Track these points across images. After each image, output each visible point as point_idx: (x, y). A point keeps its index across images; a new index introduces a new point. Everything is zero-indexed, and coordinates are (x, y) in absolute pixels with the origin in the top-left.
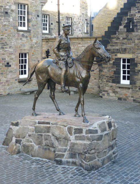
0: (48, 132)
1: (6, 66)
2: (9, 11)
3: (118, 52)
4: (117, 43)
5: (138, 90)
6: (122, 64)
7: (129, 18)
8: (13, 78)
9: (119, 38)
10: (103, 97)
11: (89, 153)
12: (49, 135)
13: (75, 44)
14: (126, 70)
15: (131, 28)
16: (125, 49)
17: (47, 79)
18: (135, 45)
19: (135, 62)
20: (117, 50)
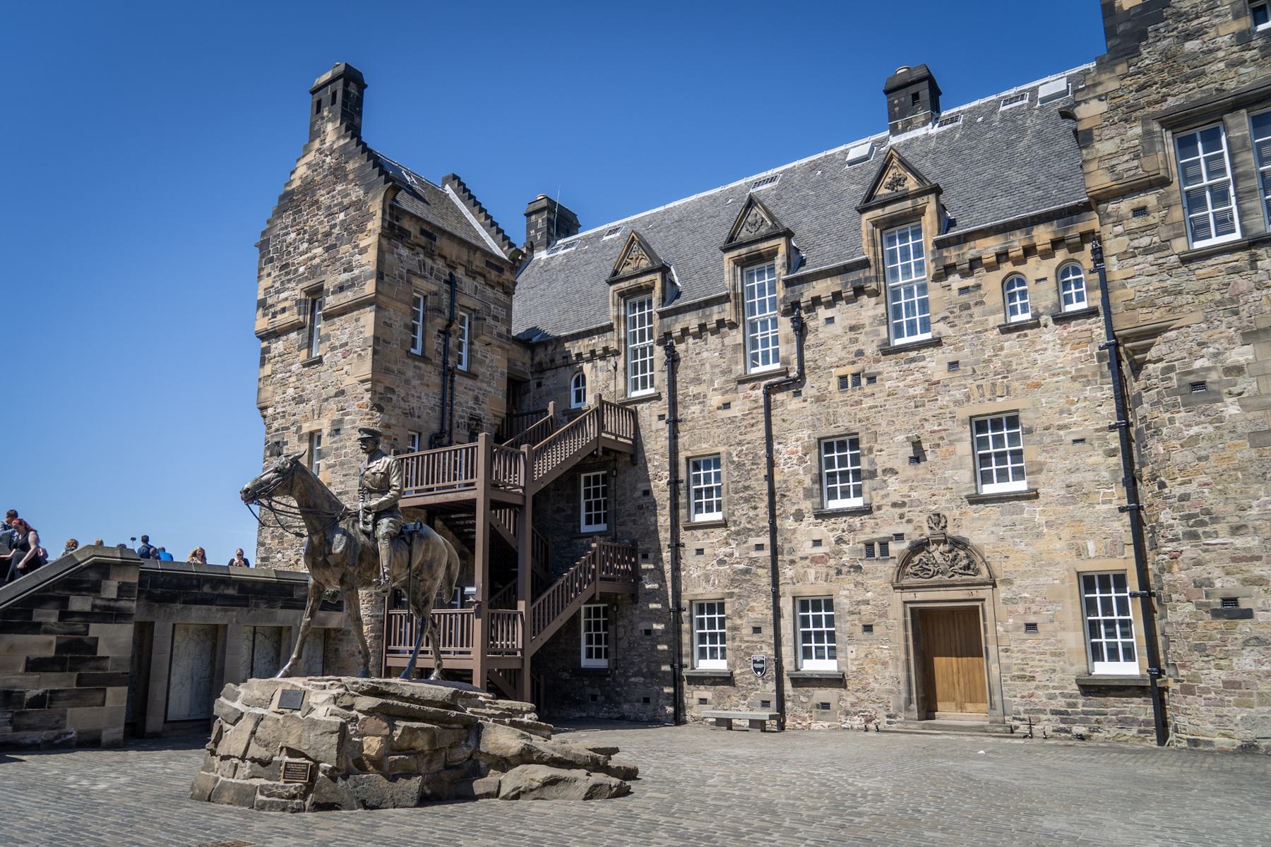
1: (1216, 614)
2: (1213, 376)
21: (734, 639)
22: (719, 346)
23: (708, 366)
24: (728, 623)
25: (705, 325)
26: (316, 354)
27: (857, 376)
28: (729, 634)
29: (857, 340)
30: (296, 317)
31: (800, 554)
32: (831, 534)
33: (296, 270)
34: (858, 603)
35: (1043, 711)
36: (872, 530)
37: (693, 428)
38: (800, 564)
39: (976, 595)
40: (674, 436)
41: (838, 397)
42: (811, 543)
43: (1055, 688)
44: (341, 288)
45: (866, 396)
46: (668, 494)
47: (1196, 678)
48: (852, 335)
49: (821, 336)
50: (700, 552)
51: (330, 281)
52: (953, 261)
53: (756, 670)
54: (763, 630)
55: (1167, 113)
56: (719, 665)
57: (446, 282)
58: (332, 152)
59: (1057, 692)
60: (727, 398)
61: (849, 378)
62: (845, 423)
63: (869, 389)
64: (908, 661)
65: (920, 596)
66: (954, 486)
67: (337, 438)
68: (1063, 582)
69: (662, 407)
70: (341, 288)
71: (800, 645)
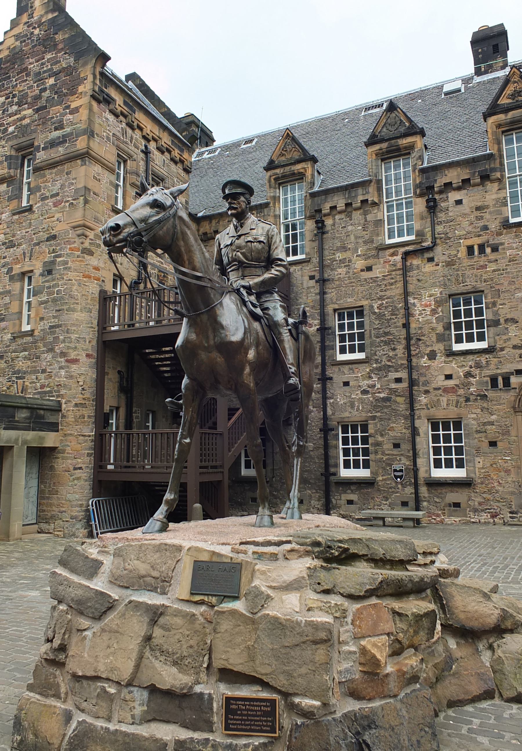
21: (376, 452)
22: (362, 222)
23: (352, 237)
24: (371, 440)
25: (351, 204)
26: (24, 204)
27: (482, 248)
28: (371, 449)
29: (482, 217)
30: (6, 171)
31: (434, 385)
33: (6, 130)
34: (484, 424)
36: (495, 367)
37: (339, 286)
38: (433, 393)
40: (323, 293)
41: (467, 262)
42: (443, 377)
44: (53, 144)
45: (490, 262)
46: (318, 338)
48: (478, 213)
49: (450, 214)
50: (346, 384)
51: (40, 140)
53: (396, 477)
54: (403, 446)
56: (363, 473)
57: (142, 151)
58: (40, 24)
60: (370, 262)
61: (476, 248)
62: (470, 284)
63: (492, 257)
67: (50, 277)
69: (309, 269)
70: (53, 144)
71: (432, 457)
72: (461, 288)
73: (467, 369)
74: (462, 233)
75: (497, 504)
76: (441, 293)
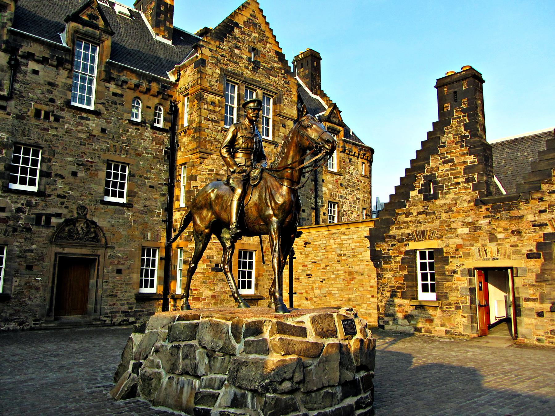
0: (193, 338)
1: (213, 270)
3: (411, 240)
4: (407, 222)
5: (453, 311)
6: (418, 261)
7: (427, 175)
8: (225, 292)
9: (412, 213)
10: (386, 327)
11: (275, 391)
12: (191, 346)
13: (337, 235)
14: (427, 273)
15: (432, 192)
16: (423, 232)
17: (210, 222)
18: (441, 222)
19: (444, 255)
20: (409, 234)
29: (52, 92)
32: (13, 205)
34: (26, 251)
35: (118, 312)
39: (96, 253)
41: (34, 121)
43: (125, 300)
45: (52, 127)
47: (201, 294)
48: (49, 87)
52: (115, 77)
55: (228, 71)
59: (126, 302)
61: (43, 112)
62: (34, 138)
63: (54, 124)
64: (52, 287)
65: (66, 250)
66: (94, 193)
68: (136, 250)
72: (25, 140)
73: (19, 205)
74: (35, 97)
75: (26, 315)
76: (8, 138)
